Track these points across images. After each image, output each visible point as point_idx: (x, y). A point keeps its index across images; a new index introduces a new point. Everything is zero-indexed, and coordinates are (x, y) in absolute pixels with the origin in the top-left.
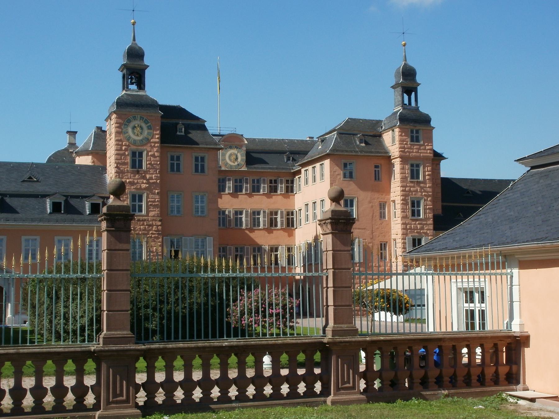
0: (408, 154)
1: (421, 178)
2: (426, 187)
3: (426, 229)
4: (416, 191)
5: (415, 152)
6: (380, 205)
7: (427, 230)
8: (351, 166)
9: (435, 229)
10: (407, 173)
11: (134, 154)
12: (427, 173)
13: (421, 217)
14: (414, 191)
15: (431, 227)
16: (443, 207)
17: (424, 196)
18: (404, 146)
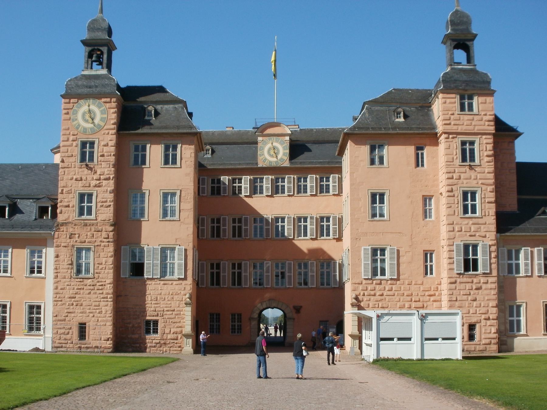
1: (477, 161)
12: (485, 154)
16: (519, 201)
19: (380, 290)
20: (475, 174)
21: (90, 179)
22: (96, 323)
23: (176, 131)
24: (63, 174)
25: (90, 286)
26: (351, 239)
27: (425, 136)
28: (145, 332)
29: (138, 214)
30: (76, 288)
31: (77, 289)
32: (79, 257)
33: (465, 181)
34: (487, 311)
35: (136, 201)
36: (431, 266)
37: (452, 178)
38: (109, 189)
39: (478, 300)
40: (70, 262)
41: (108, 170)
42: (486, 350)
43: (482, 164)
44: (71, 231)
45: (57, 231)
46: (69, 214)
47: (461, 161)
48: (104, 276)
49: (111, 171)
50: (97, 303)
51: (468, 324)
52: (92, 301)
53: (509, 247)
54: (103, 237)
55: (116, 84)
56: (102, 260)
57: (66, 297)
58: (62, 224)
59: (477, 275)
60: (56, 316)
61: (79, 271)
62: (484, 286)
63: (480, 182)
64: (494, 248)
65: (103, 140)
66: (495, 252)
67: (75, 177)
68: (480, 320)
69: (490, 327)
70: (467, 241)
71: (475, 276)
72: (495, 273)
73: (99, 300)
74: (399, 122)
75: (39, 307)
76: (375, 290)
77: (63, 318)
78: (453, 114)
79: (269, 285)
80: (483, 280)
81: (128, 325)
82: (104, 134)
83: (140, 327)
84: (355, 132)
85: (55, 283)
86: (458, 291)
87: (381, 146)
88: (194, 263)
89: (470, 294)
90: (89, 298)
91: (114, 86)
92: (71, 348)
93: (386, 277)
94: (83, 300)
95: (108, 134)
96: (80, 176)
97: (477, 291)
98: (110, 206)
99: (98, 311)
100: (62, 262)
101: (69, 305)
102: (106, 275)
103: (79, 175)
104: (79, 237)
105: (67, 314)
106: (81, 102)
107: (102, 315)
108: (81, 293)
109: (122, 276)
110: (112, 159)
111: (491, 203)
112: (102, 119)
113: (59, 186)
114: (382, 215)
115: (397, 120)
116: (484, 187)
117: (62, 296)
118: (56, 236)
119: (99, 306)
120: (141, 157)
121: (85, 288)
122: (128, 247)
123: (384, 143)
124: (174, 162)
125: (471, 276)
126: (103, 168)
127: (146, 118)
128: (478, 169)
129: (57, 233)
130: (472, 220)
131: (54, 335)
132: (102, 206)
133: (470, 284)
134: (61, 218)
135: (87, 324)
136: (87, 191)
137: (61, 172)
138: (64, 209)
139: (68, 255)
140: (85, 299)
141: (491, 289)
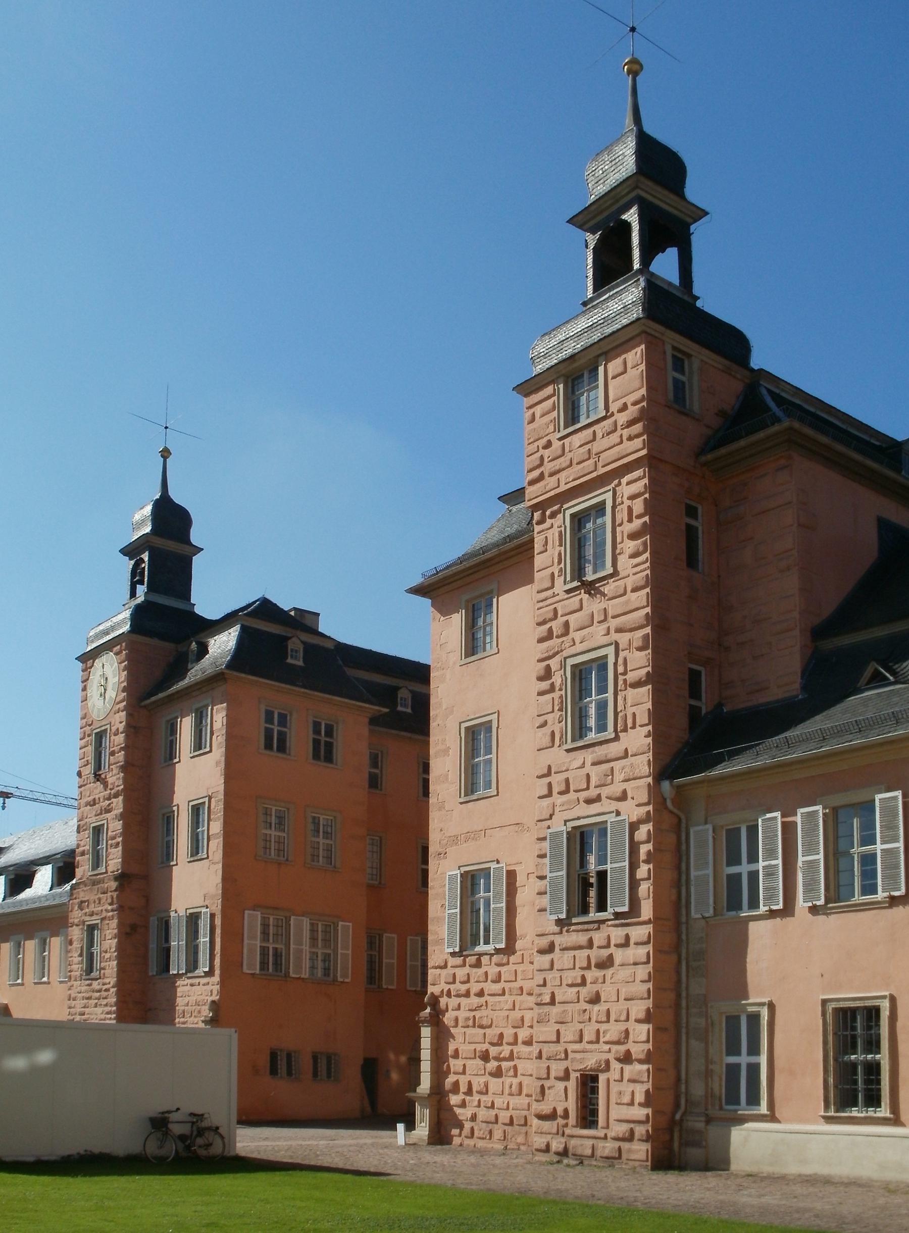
19: (477, 982)
20: (603, 605)
33: (577, 636)
34: (623, 1035)
37: (549, 635)
39: (603, 999)
42: (620, 1157)
43: (619, 568)
47: (568, 579)
51: (578, 1074)
53: (726, 820)
59: (604, 922)
62: (619, 956)
63: (613, 623)
64: (642, 832)
66: (648, 841)
68: (607, 1062)
69: (632, 1086)
70: (579, 818)
71: (596, 926)
72: (647, 910)
76: (468, 981)
78: (549, 445)
80: (617, 934)
86: (558, 975)
89: (583, 983)
97: (599, 973)
111: (637, 685)
116: (623, 639)
125: (586, 927)
128: (609, 588)
130: (593, 752)
133: (585, 953)
141: (635, 964)
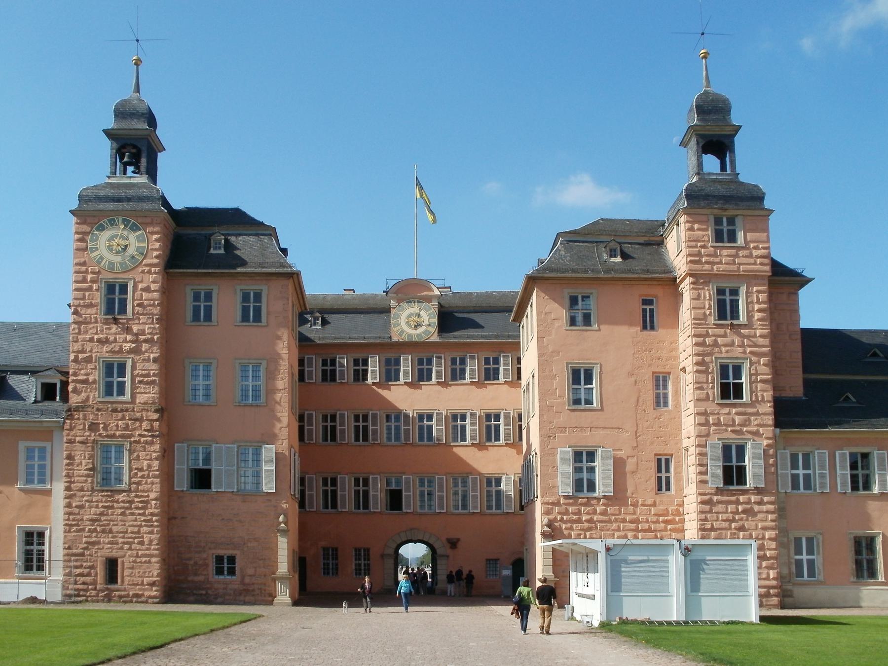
0: (707, 267)
2: (755, 336)
3: (757, 425)
4: (732, 344)
5: (726, 264)
6: (657, 379)
7: (759, 425)
8: (588, 302)
9: (778, 424)
10: (707, 307)
11: (110, 288)
13: (744, 400)
14: (725, 345)
15: (770, 420)
17: (749, 355)
18: (699, 251)
21: (121, 341)
22: (134, 559)
23: (259, 270)
24: (77, 331)
25: (123, 502)
26: (541, 437)
27: (655, 283)
28: (214, 573)
29: (201, 396)
30: (101, 505)
31: (103, 507)
32: (106, 459)
35: (197, 376)
36: (668, 479)
38: (152, 356)
40: (90, 466)
41: (151, 328)
44: (91, 418)
45: (67, 419)
46: (87, 394)
48: (146, 487)
49: (154, 328)
50: (136, 529)
52: (127, 524)
53: (794, 450)
54: (143, 429)
55: (161, 196)
56: (143, 463)
57: (85, 518)
58: (77, 409)
60: (69, 548)
61: (106, 480)
65: (142, 282)
67: (96, 337)
73: (139, 523)
74: (614, 262)
75: (41, 535)
77: (80, 551)
79: (410, 509)
81: (187, 562)
82: (143, 272)
83: (207, 565)
84: (546, 275)
85: (65, 498)
87: (585, 298)
88: (292, 471)
90: (121, 521)
91: (159, 199)
92: (94, 596)
93: (596, 494)
94: (112, 523)
95: (149, 272)
96: (105, 336)
98: (153, 382)
99: (136, 541)
100: (78, 466)
101: (88, 532)
102: (149, 486)
103: (103, 334)
104: (105, 428)
105: (86, 545)
106: (104, 222)
107: (144, 547)
108: (110, 513)
109: (176, 489)
110: (157, 310)
112: (138, 249)
113: (71, 350)
114: (589, 402)
115: (613, 260)
117: (78, 517)
118: (67, 427)
119: (139, 532)
120: (205, 310)
121: (116, 505)
122: (186, 445)
123: (592, 293)
124: (258, 318)
126: (142, 324)
127: (212, 251)
129: (68, 421)
131: (65, 577)
132: (140, 382)
134: (74, 399)
135: (120, 561)
136: (117, 358)
137: (74, 329)
138: (79, 386)
139: (87, 455)
140: (115, 523)
